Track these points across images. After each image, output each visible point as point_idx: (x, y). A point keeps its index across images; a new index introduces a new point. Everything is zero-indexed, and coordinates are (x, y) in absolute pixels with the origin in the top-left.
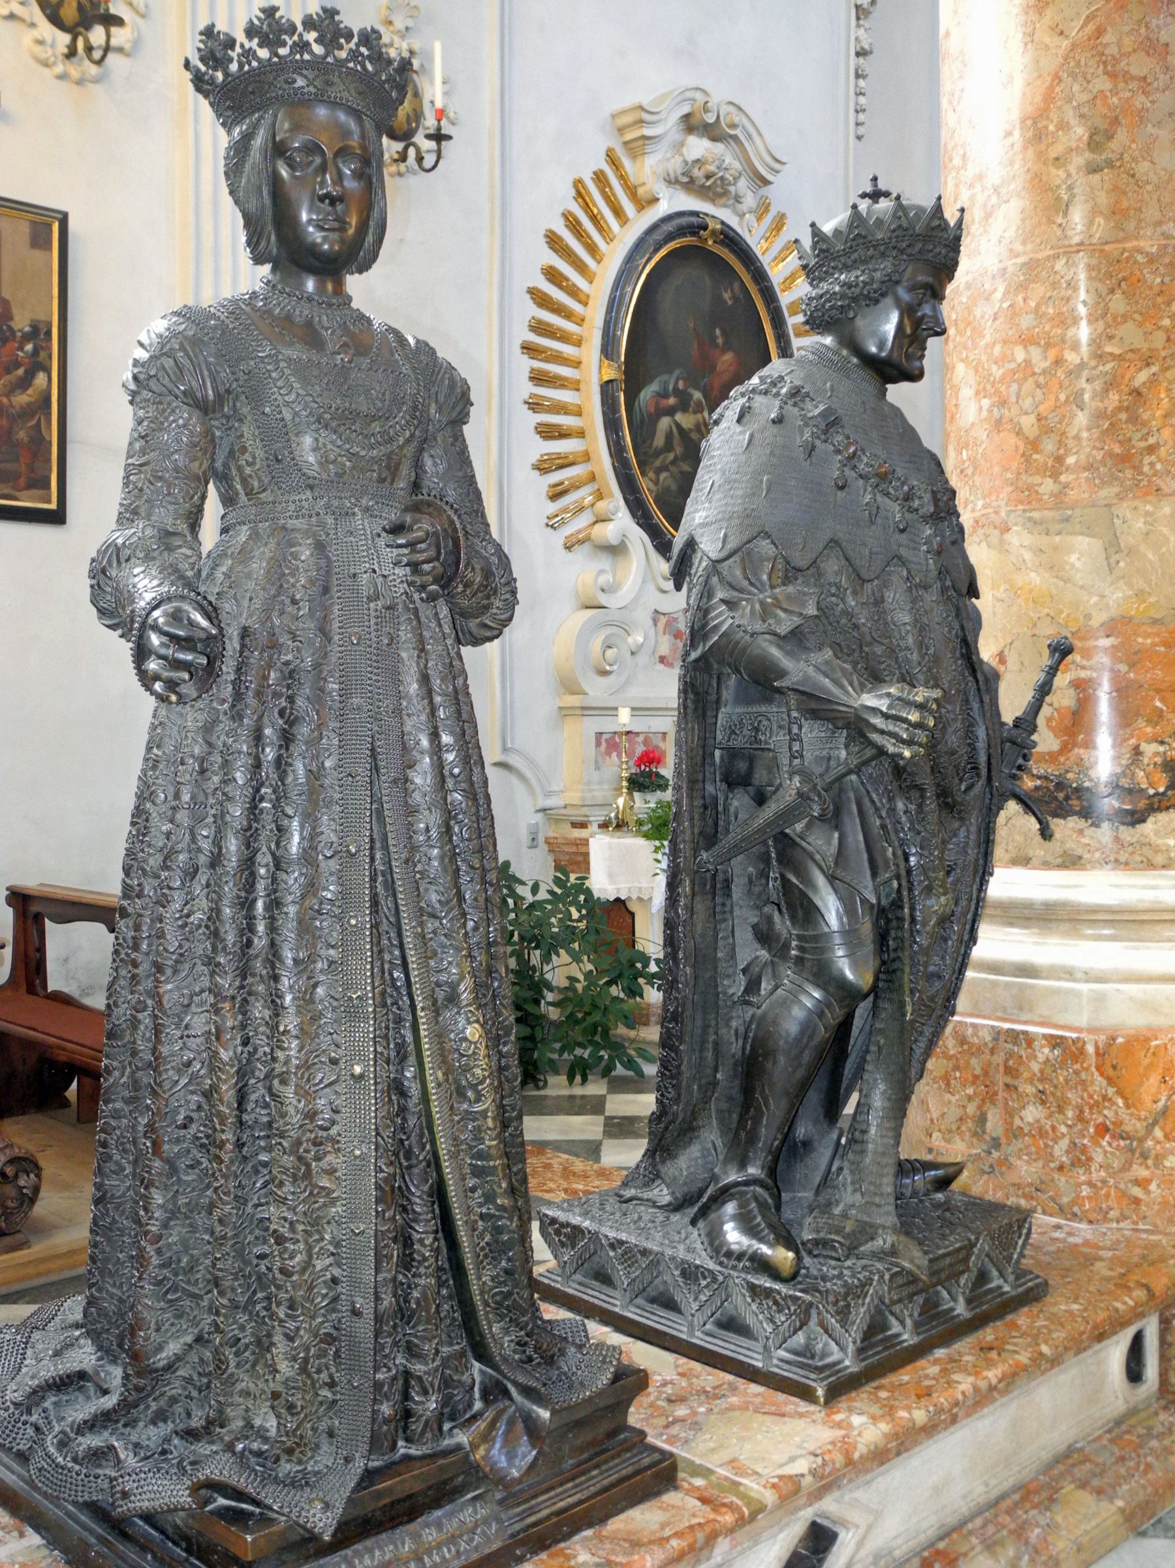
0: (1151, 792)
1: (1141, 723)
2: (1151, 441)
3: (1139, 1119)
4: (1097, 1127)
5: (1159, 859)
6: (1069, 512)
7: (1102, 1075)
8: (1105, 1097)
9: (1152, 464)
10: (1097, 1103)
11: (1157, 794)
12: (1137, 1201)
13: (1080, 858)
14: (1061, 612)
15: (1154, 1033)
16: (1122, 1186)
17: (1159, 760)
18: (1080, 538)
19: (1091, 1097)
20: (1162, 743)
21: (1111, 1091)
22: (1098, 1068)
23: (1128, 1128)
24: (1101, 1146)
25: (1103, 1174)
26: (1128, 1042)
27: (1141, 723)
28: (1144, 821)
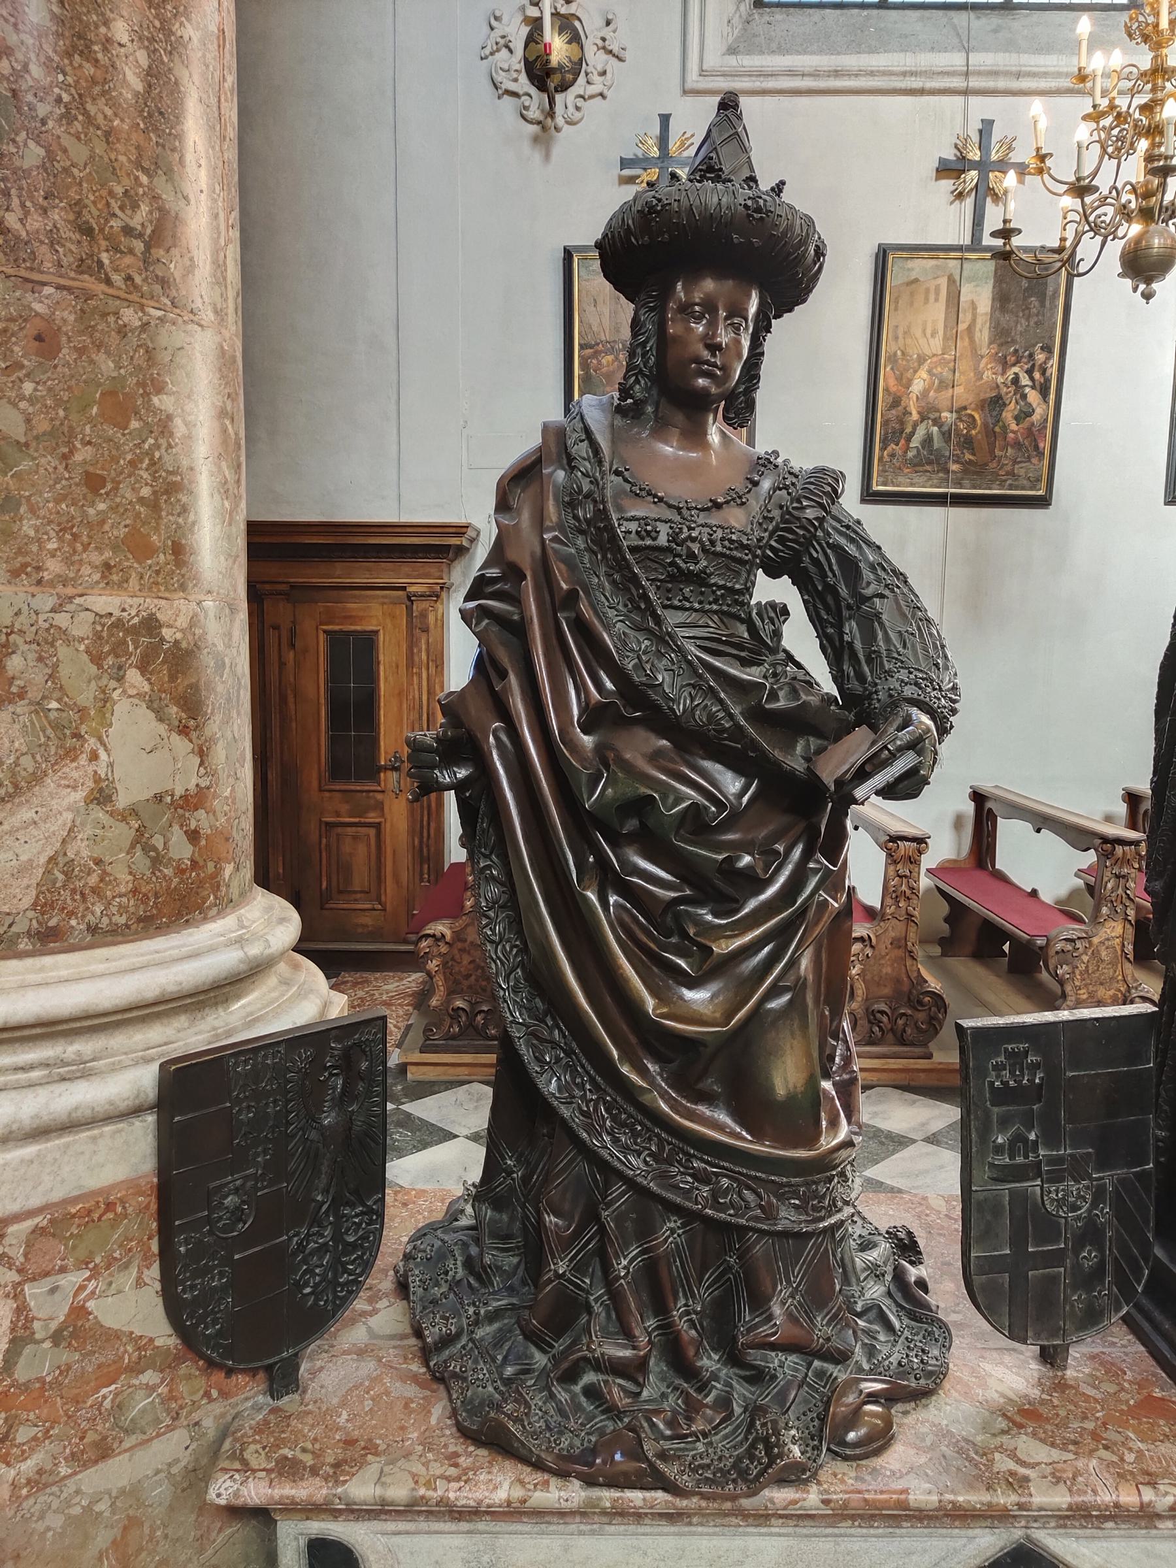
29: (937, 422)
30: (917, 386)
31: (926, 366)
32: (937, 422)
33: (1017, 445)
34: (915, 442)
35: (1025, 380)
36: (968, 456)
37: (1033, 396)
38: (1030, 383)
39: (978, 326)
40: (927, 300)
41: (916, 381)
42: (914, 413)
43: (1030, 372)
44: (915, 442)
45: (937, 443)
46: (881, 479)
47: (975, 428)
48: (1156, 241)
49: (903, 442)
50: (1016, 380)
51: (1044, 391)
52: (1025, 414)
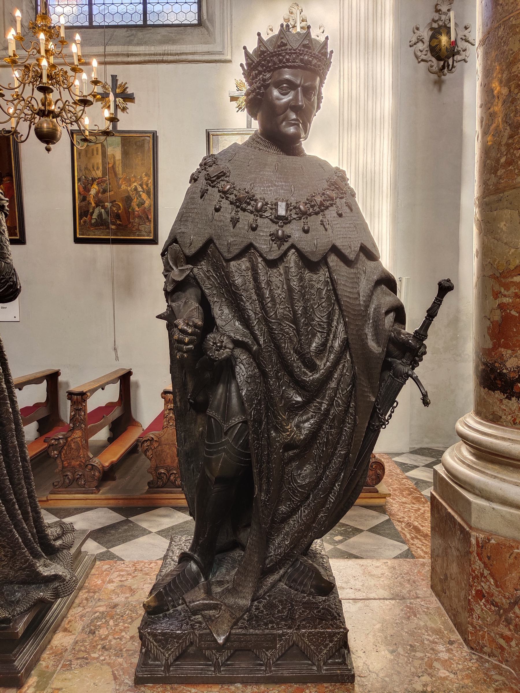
3: (505, 597)
4: (477, 591)
6: (501, 195)
7: (480, 559)
8: (482, 574)
10: (477, 576)
12: (502, 648)
13: (501, 417)
14: (495, 260)
16: (492, 634)
18: (506, 211)
19: (474, 571)
21: (486, 572)
22: (478, 555)
23: (497, 600)
24: (479, 605)
25: (480, 622)
26: (498, 544)
29: (103, 207)
30: (93, 192)
31: (95, 183)
32: (103, 207)
33: (139, 217)
34: (95, 216)
35: (140, 189)
36: (118, 222)
37: (144, 196)
38: (141, 190)
39: (117, 165)
40: (93, 154)
41: (92, 190)
42: (93, 203)
43: (141, 185)
44: (95, 216)
45: (104, 216)
46: (81, 233)
47: (120, 209)
48: (45, 125)
49: (89, 216)
50: (136, 189)
51: (148, 193)
52: (141, 204)
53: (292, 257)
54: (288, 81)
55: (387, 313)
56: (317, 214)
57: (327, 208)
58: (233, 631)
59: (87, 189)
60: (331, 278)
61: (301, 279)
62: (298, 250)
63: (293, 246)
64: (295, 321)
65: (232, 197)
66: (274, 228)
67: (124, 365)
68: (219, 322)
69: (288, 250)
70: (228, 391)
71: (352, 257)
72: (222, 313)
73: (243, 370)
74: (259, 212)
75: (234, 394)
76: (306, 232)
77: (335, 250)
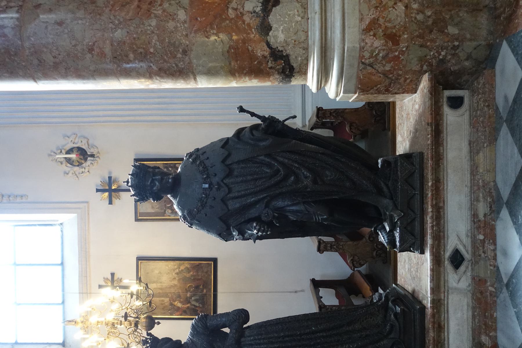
0: (283, 64)
1: (262, 67)
2: (174, 65)
5: (305, 62)
8: (377, 90)
9: (181, 65)
11: (284, 63)
12: (411, 81)
15: (358, 77)
17: (273, 63)
20: (268, 62)
21: (375, 88)
23: (388, 84)
26: (360, 84)
27: (262, 67)
28: (293, 66)
29: (191, 298)
30: (179, 305)
36: (201, 287)
44: (197, 305)
45: (197, 298)
53: (226, 181)
54: (151, 183)
55: (253, 135)
56: (207, 170)
57: (205, 165)
58: (399, 208)
59: (178, 309)
60: (236, 163)
61: (237, 177)
62: (224, 178)
63: (222, 181)
64: (256, 180)
65: (200, 208)
66: (214, 189)
67: (307, 285)
68: (257, 215)
69: (224, 183)
70: (289, 211)
71: (226, 153)
72: (253, 213)
73: (280, 203)
74: (207, 196)
75: (291, 208)
76: (216, 175)
77: (223, 161)
